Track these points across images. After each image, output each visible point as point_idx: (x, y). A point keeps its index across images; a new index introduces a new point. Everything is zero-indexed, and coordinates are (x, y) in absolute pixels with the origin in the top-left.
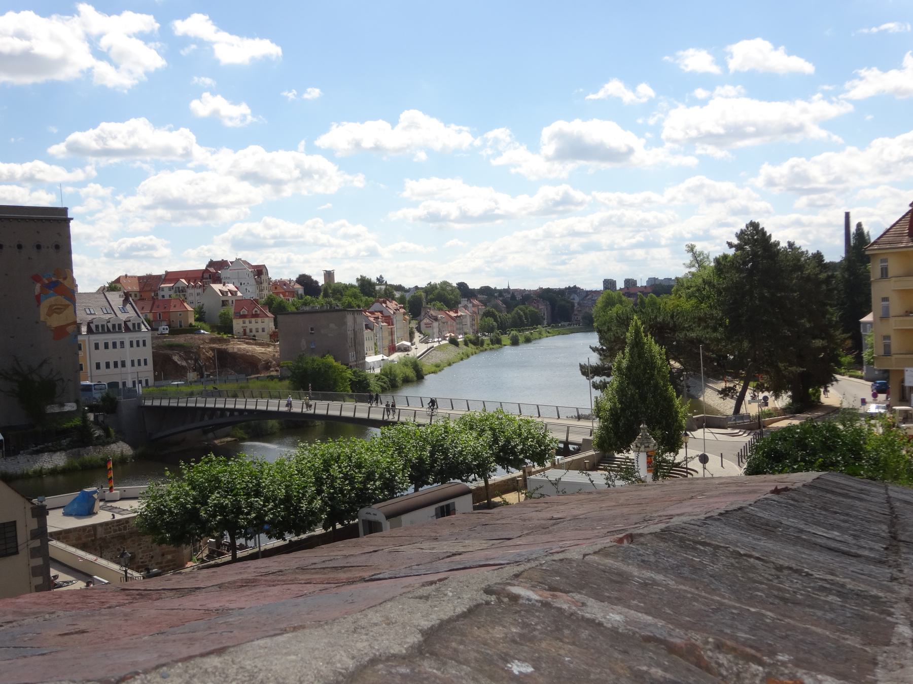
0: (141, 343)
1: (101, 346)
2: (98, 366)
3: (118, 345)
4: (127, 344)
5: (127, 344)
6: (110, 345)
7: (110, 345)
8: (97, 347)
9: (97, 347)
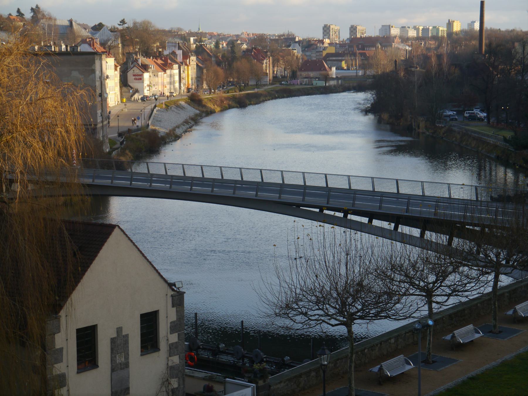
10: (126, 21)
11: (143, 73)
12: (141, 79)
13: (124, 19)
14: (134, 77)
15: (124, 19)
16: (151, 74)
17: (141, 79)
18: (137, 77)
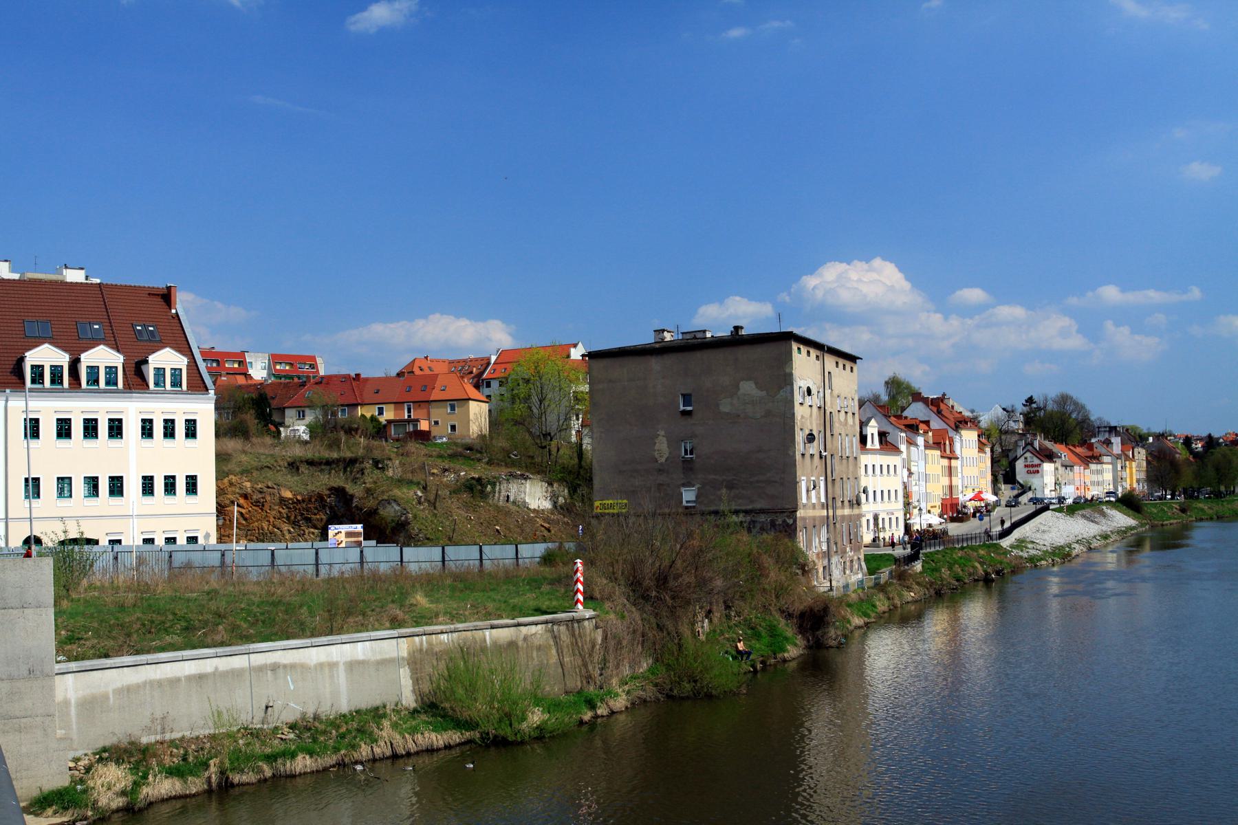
0: (180, 429)
1: (48, 428)
2: (33, 486)
3: (103, 429)
4: (132, 428)
5: (132, 428)
6: (77, 429)
7: (77, 429)
8: (33, 428)
9: (33, 428)
10: (1036, 398)
11: (1042, 461)
12: (1038, 472)
13: (1032, 397)
14: (1027, 469)
15: (1032, 397)
16: (1058, 465)
17: (1038, 472)
18: (1031, 469)
